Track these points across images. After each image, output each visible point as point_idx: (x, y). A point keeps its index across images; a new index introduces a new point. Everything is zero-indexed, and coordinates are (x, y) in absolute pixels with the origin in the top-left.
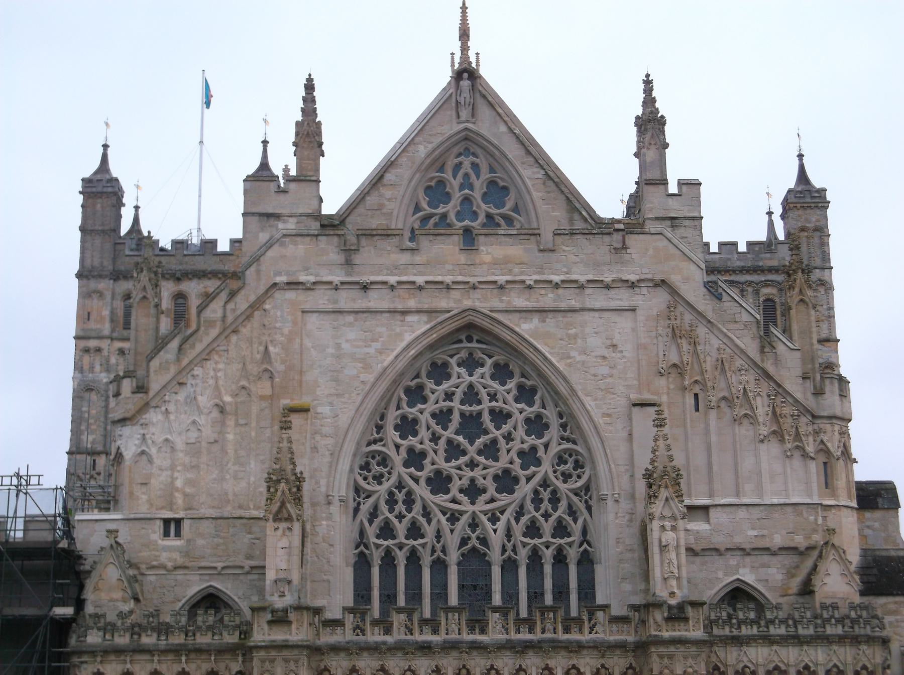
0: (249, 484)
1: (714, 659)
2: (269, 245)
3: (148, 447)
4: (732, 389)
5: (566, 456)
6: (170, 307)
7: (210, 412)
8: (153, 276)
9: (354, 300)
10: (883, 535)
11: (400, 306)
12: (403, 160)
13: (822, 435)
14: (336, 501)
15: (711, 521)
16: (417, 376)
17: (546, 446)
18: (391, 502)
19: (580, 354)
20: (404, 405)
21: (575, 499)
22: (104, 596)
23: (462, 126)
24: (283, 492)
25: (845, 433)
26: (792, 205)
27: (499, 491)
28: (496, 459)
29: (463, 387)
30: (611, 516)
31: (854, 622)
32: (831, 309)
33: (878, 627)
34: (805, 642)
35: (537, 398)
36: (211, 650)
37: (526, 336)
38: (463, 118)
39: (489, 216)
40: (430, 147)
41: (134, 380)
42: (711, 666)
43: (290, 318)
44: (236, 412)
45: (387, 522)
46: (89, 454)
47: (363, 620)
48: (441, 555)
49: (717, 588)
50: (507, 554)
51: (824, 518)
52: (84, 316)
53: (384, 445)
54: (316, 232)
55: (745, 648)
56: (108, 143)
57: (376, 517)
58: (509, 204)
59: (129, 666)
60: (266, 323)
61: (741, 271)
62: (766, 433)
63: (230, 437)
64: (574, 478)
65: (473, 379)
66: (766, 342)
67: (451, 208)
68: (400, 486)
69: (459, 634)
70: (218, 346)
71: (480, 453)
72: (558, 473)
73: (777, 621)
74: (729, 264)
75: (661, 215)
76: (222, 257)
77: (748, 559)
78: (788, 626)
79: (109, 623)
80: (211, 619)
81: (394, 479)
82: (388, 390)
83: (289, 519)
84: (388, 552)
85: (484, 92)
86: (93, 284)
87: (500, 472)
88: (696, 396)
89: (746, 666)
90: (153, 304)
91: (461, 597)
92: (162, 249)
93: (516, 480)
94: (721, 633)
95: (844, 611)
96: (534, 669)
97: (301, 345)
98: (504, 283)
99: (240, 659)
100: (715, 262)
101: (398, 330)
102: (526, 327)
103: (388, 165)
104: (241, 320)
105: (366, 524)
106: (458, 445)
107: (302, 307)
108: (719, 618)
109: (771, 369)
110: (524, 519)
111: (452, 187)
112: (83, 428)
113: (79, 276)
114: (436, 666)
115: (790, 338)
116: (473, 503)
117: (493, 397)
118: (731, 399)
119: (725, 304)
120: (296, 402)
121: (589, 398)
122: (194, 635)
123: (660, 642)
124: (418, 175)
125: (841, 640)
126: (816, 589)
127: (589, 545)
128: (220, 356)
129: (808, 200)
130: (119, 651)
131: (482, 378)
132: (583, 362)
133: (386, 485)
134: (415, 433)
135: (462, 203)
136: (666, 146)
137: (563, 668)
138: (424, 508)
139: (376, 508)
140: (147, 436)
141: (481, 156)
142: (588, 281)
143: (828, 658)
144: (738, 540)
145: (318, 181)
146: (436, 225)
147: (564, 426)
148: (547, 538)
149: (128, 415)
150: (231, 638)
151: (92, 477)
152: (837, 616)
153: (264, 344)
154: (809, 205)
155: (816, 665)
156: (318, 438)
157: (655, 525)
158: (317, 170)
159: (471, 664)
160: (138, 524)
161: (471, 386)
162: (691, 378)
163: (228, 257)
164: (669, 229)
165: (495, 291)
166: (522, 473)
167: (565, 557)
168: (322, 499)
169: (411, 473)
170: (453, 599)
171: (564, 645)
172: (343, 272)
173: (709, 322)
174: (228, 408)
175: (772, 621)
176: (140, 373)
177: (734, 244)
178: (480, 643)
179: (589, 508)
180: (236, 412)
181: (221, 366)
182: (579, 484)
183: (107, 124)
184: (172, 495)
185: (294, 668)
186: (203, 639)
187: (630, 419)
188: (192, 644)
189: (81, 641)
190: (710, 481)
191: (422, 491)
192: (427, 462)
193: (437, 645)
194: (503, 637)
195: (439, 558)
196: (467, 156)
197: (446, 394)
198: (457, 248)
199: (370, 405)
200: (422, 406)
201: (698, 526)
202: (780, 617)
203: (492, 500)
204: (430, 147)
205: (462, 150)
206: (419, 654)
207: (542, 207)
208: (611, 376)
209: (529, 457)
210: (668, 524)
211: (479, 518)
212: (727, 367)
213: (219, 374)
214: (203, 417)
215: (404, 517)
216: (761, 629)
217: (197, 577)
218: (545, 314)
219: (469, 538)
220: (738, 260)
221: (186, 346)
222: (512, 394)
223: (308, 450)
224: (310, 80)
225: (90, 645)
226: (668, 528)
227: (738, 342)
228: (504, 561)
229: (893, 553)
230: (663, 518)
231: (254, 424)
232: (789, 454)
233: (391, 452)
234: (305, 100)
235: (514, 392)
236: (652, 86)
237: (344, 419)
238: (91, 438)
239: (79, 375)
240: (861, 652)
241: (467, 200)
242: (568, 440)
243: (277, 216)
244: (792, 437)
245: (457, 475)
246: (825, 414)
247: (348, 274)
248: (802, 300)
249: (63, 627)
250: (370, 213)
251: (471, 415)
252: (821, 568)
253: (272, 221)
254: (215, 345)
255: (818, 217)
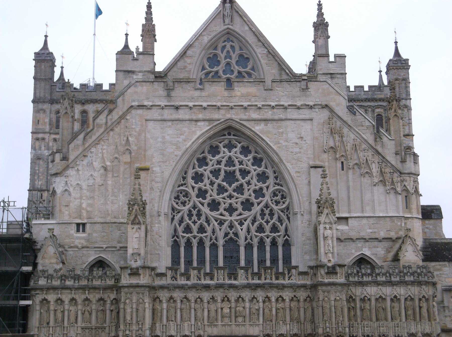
0: (119, 206)
1: (350, 292)
2: (129, 87)
3: (68, 187)
4: (360, 159)
5: (278, 193)
6: (79, 117)
7: (99, 170)
8: (70, 102)
9: (171, 114)
10: (434, 232)
11: (194, 118)
12: (196, 44)
13: (405, 182)
14: (162, 215)
15: (349, 225)
16: (203, 152)
17: (267, 187)
18: (190, 215)
19: (284, 142)
20: (197, 167)
21: (282, 214)
22: (47, 261)
23: (226, 27)
24: (136, 210)
25: (416, 182)
26: (391, 67)
27: (244, 209)
28: (242, 194)
29: (226, 158)
30: (299, 222)
31: (419, 274)
32: (410, 119)
33: (431, 277)
34: (395, 284)
36: (100, 288)
37: (258, 133)
38: (226, 23)
39: (239, 72)
40: (210, 37)
41: (61, 154)
42: (348, 296)
43: (139, 123)
44: (113, 169)
45: (188, 225)
46: (39, 191)
47: (176, 273)
48: (215, 241)
49: (352, 258)
50: (247, 241)
51: (405, 223)
52: (36, 122)
53: (186, 187)
54: (153, 80)
55: (365, 287)
56: (47, 35)
57: (183, 222)
58: (250, 67)
59: (60, 296)
60: (128, 126)
61: (365, 101)
62: (377, 181)
63: (110, 183)
64: (281, 203)
65: (231, 154)
66: (378, 136)
67: (220, 68)
68: (194, 207)
69: (224, 280)
70: (103, 137)
71: (234, 191)
72: (273, 201)
73: (381, 274)
74: (359, 97)
75: (326, 72)
76: (105, 92)
77: (367, 244)
78: (386, 276)
79: (50, 275)
80: (100, 273)
81: (191, 204)
82: (188, 159)
83: (139, 223)
84: (188, 240)
85: (237, 9)
86: (40, 106)
87: (244, 200)
88: (342, 162)
89: (365, 296)
90: (70, 116)
91: (224, 262)
92: (75, 89)
93: (252, 204)
94: (353, 280)
95: (414, 269)
96: (261, 297)
97: (145, 137)
98: (247, 106)
99: (115, 292)
100: (352, 96)
101: (194, 129)
102: (258, 128)
103: (189, 46)
104: (115, 124)
105: (178, 226)
106: (224, 187)
107: (146, 118)
108: (353, 272)
109: (380, 150)
110: (256, 224)
111: (221, 58)
112: (36, 178)
113: (33, 101)
114: (212, 296)
115: (390, 134)
116: (231, 216)
117: (241, 163)
118: (360, 164)
119: (357, 117)
120: (143, 165)
121: (289, 164)
122: (92, 281)
123: (323, 284)
124: (203, 52)
125: (412, 283)
126: (401, 258)
127: (288, 236)
128: (104, 142)
129: (400, 65)
130: (55, 288)
131: (235, 153)
132: (286, 146)
133: (188, 207)
134: (202, 181)
135: (226, 66)
136: (329, 37)
137: (275, 297)
138: (207, 218)
139: (182, 218)
140: (68, 182)
141: (236, 42)
142: (289, 105)
143: (406, 292)
144: (363, 234)
145: (153, 55)
146: (213, 77)
147: (276, 178)
148: (268, 233)
149: (58, 172)
150: (110, 282)
151: (40, 202)
152: (411, 271)
153: (126, 136)
154: (400, 67)
155: (400, 295)
156: (153, 183)
157: (321, 227)
158: (153, 49)
159: (229, 295)
160: (64, 226)
161: (230, 158)
162: (340, 154)
163: (108, 92)
164: (330, 79)
165: (242, 110)
166: (255, 201)
167: (277, 243)
168: (155, 214)
169: (200, 201)
170: (221, 263)
171: (275, 286)
172: (166, 100)
173: (349, 126)
174: (108, 168)
175: (379, 274)
176: (64, 150)
177: (362, 87)
178: (234, 285)
179: (288, 218)
180: (113, 169)
181: (105, 147)
182: (284, 206)
183: (47, 25)
184: (80, 211)
185: (142, 297)
186: (97, 283)
187: (309, 174)
188: (91, 285)
189: (36, 283)
190: (349, 205)
191: (205, 210)
192: (208, 195)
193: (213, 286)
194: (245, 282)
195: (214, 243)
196: (229, 42)
197: (218, 161)
198: (223, 89)
199: (179, 167)
200: (206, 168)
201: (343, 227)
202: (382, 272)
203: (240, 214)
204: (210, 37)
205: (226, 39)
206: (204, 290)
207: (266, 68)
208: (300, 153)
209: (259, 193)
210: (328, 226)
211: (233, 223)
212: (358, 149)
213: (104, 151)
214: (96, 172)
215: (196, 222)
216: (373, 278)
217: (94, 252)
218: (267, 122)
219: (229, 233)
220: (364, 95)
221: (88, 137)
222: (250, 162)
223: (149, 189)
224: (149, 3)
225: (41, 286)
226: (328, 228)
227: (364, 136)
228: (246, 244)
229: (439, 241)
230: (325, 223)
231: (121, 176)
232: (388, 192)
233: (190, 190)
234: (147, 13)
235: (252, 160)
236: (322, 7)
237: (167, 174)
238: (40, 183)
239: (34, 152)
240: (422, 289)
241: (228, 64)
242: (278, 185)
243: (133, 72)
244: (390, 183)
245: (223, 201)
246: (406, 172)
247: (169, 101)
248: (396, 115)
249: (27, 277)
250: (179, 70)
251: (230, 172)
252: (403, 248)
253: (130, 74)
254: (102, 136)
255: (404, 73)
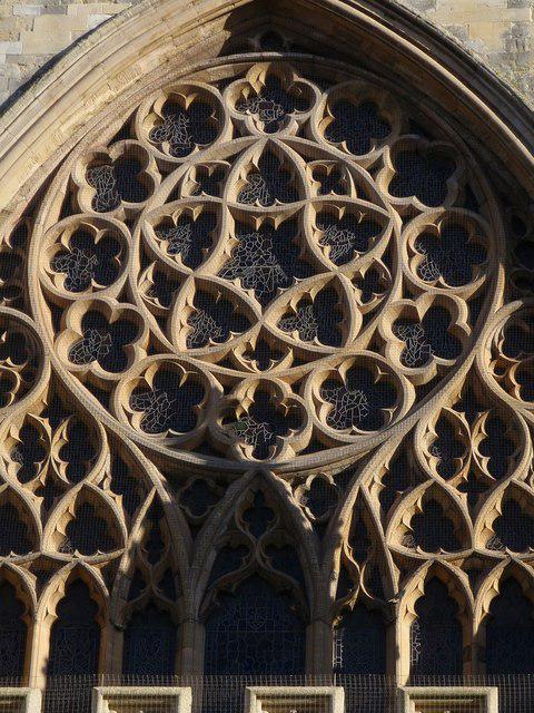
29: (254, 155)
35: (453, 184)
65: (276, 137)
203: (318, 443)
219: (245, 548)
251: (268, 225)
